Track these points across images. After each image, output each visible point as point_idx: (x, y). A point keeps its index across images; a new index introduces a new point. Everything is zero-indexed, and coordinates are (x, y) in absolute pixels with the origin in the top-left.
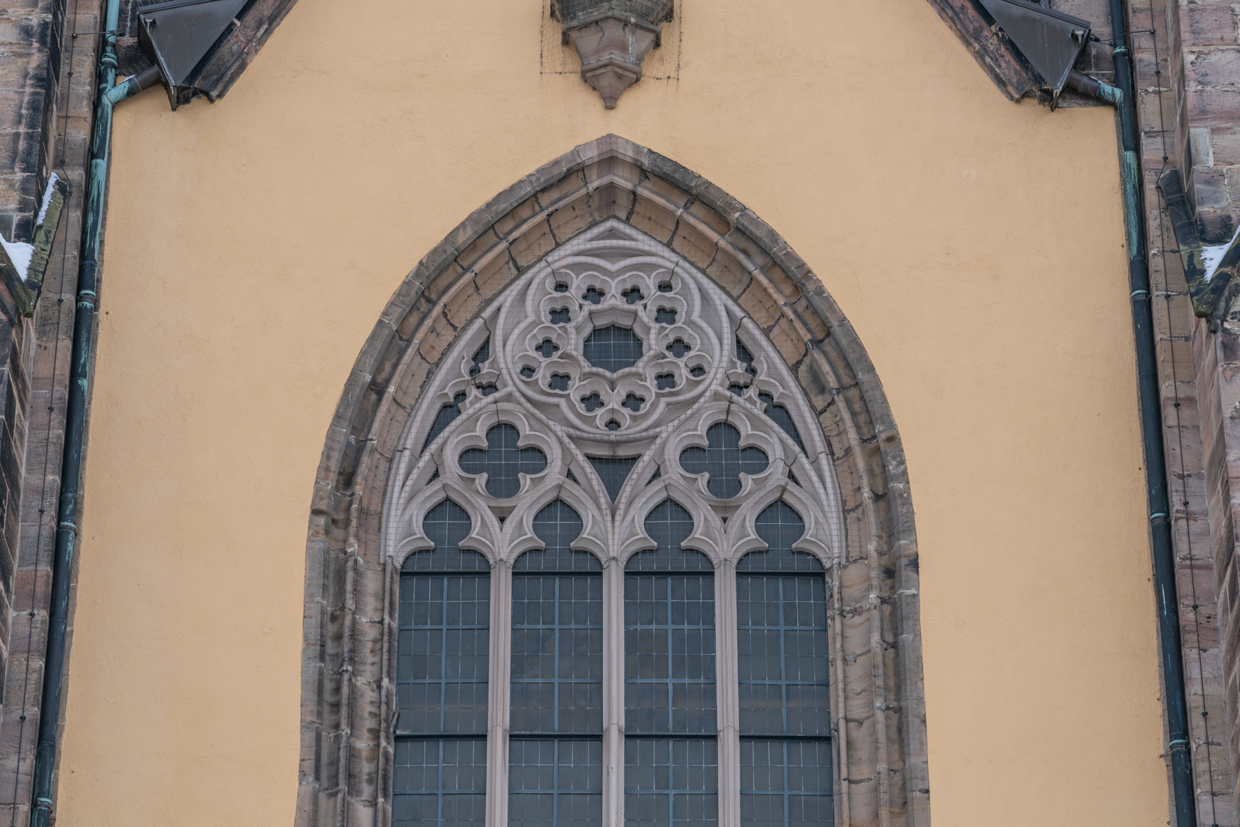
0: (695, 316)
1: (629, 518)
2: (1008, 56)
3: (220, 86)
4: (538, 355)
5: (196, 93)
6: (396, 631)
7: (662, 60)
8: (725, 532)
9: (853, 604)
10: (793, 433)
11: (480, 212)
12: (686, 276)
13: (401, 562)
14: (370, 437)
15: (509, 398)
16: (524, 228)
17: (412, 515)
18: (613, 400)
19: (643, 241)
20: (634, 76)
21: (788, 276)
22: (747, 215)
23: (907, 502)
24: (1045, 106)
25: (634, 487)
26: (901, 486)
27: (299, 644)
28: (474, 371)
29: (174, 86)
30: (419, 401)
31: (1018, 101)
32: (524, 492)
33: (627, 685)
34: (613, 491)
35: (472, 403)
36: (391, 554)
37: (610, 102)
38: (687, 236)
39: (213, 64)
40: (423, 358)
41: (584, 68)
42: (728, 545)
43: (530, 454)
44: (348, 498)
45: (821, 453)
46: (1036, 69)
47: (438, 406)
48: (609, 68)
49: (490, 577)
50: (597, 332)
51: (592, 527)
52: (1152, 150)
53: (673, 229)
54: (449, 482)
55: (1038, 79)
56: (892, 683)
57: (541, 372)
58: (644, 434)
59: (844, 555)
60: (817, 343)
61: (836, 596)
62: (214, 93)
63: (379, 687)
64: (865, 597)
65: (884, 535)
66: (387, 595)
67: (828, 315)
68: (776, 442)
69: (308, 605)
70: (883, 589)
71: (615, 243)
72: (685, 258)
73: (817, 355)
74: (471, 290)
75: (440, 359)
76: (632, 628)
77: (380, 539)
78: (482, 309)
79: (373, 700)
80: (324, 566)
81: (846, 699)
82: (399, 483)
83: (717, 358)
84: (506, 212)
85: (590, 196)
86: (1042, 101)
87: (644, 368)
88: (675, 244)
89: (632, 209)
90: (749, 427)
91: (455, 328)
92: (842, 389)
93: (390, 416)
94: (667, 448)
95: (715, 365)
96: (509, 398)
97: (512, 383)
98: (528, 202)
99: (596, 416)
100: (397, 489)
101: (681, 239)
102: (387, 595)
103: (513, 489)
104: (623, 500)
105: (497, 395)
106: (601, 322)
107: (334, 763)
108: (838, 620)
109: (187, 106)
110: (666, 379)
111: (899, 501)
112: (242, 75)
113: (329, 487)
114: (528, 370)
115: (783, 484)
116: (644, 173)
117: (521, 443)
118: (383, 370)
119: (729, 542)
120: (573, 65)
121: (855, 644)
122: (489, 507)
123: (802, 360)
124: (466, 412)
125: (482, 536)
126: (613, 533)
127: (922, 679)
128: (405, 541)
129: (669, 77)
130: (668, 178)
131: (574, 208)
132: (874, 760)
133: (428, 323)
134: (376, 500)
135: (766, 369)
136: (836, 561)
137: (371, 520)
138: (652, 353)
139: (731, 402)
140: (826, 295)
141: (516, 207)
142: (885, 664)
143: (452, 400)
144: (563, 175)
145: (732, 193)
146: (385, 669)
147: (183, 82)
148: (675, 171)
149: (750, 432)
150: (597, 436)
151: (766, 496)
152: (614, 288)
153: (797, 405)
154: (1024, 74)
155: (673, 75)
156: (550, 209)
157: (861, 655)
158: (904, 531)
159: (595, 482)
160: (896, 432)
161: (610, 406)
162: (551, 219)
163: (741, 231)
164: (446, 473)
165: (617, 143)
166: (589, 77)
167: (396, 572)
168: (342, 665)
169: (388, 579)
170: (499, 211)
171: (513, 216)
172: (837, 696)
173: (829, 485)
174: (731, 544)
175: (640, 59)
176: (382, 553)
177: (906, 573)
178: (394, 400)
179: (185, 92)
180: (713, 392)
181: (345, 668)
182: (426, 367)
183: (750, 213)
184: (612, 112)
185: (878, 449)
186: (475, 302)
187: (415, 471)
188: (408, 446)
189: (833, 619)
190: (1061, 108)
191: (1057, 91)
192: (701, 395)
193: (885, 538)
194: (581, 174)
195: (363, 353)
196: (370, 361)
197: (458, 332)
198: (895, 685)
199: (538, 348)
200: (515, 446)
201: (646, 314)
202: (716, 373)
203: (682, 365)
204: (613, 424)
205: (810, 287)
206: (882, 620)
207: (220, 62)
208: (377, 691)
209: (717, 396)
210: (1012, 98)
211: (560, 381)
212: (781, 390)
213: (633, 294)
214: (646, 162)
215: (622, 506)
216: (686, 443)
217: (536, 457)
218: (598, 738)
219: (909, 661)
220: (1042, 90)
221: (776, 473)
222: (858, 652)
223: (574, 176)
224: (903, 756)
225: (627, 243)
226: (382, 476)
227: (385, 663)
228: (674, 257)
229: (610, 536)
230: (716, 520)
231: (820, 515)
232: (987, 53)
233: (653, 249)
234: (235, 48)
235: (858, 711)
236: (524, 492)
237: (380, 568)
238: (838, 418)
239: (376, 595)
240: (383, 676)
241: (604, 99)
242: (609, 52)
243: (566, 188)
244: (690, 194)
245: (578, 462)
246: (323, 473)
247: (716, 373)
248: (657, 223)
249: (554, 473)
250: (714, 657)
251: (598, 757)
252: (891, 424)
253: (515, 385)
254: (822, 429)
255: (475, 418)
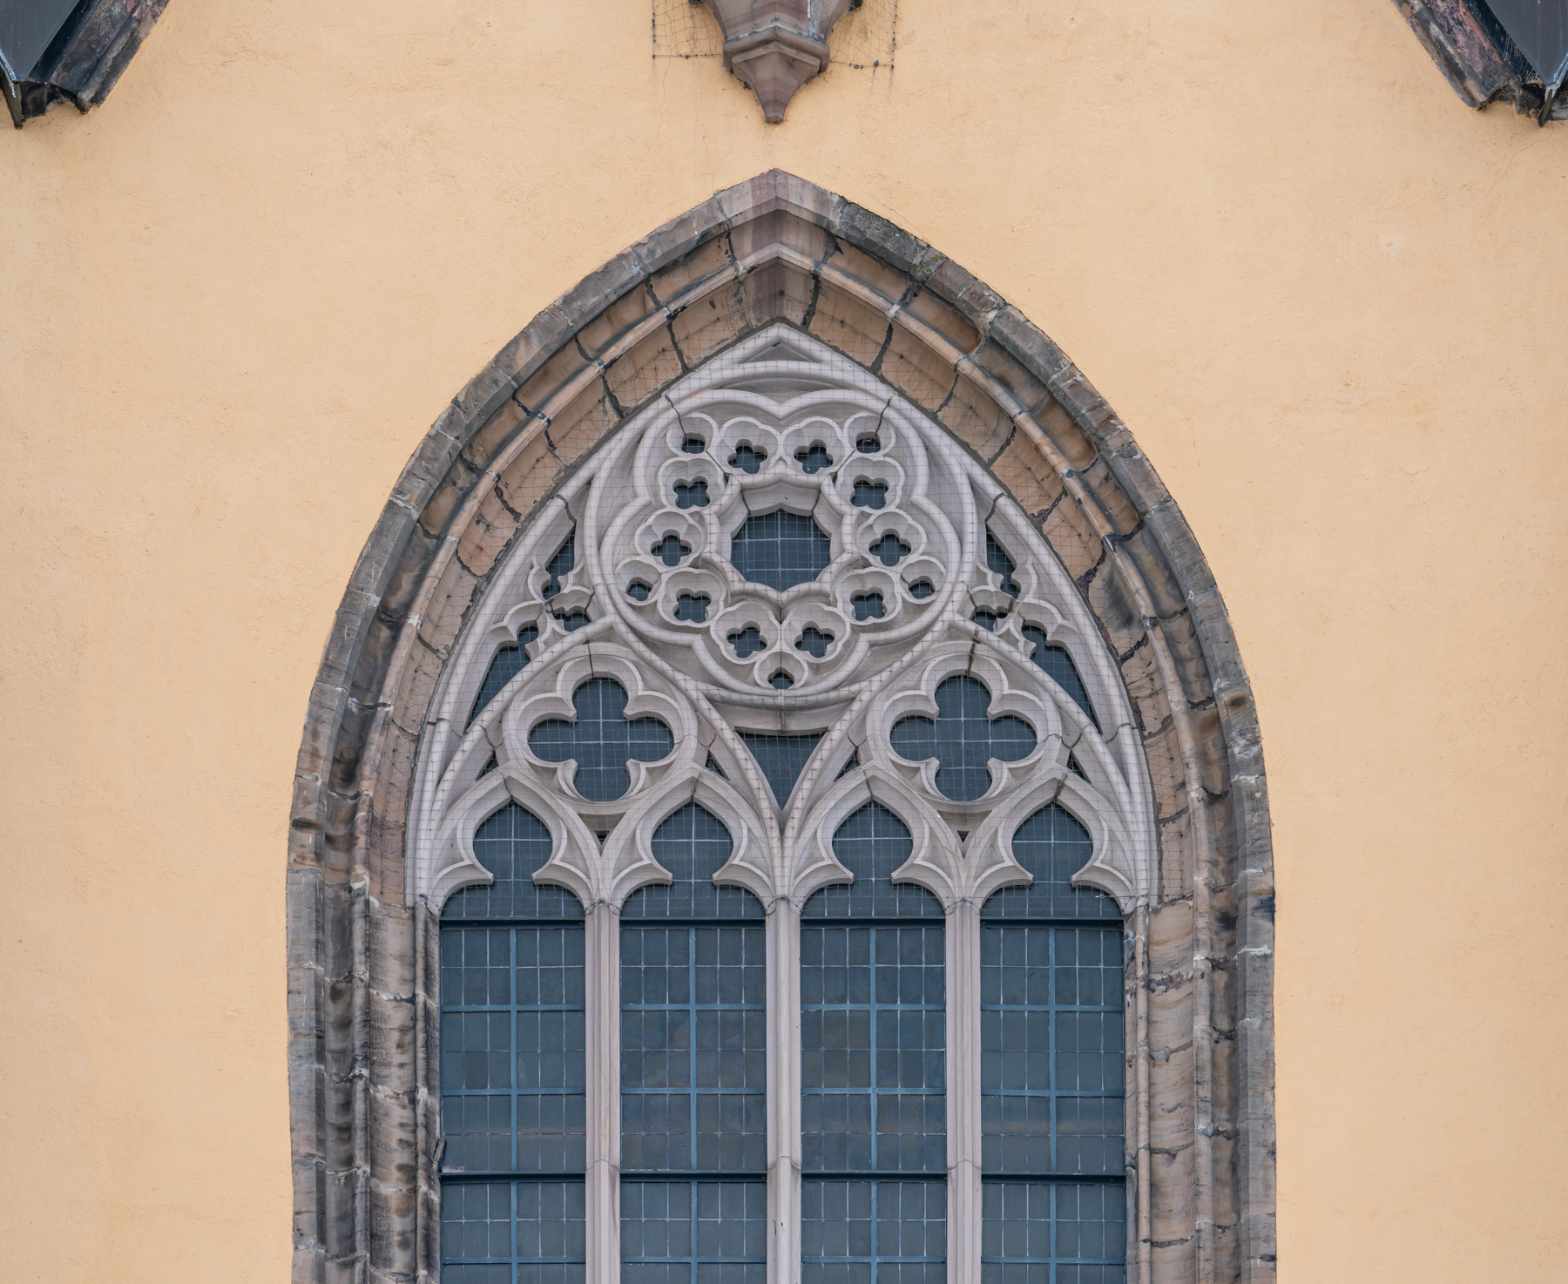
0: (919, 496)
1: (808, 833)
2: (1471, 24)
3: (96, 82)
4: (655, 562)
5: (57, 94)
6: (436, 1014)
7: (864, 31)
8: (964, 856)
9: (1167, 970)
10: (1078, 692)
11: (553, 311)
12: (903, 425)
13: (441, 905)
14: (381, 701)
15: (609, 635)
16: (629, 339)
17: (455, 829)
18: (782, 637)
19: (831, 363)
20: (816, 62)
21: (1075, 425)
22: (1009, 316)
23: (1261, 806)
24: (1528, 116)
25: (815, 782)
26: (1252, 780)
27: (283, 1035)
28: (550, 590)
29: (15, 83)
30: (461, 640)
31: (1482, 108)
32: (636, 791)
33: (806, 1098)
34: (782, 788)
35: (547, 644)
36: (423, 891)
37: (774, 110)
38: (905, 354)
39: (81, 42)
40: (464, 567)
41: (730, 46)
42: (968, 877)
43: (646, 728)
44: (351, 802)
45: (1123, 725)
46: (1517, 46)
47: (492, 648)
48: (772, 47)
49: (584, 929)
50: (754, 522)
51: (749, 847)
53: (882, 341)
54: (515, 775)
55: (1520, 66)
56: (1224, 1093)
57: (662, 589)
58: (833, 695)
59: (1155, 891)
60: (1121, 539)
61: (1140, 958)
62: (86, 96)
63: (413, 1101)
64: (1187, 959)
65: (1221, 859)
66: (420, 956)
67: (1142, 491)
68: (1049, 707)
69: (294, 973)
70: (1217, 946)
71: (783, 366)
72: (902, 393)
73: (1121, 560)
74: (541, 449)
75: (493, 569)
76: (813, 1008)
77: (405, 868)
78: (560, 483)
79: (405, 1121)
80: (317, 911)
81: (1151, 1118)
82: (432, 777)
83: (954, 567)
84: (597, 312)
85: (741, 283)
86: (1525, 107)
87: (833, 583)
88: (887, 368)
89: (813, 306)
90: (1006, 683)
91: (516, 515)
92: (1160, 618)
93: (413, 666)
94: (869, 717)
95: (951, 577)
96: (609, 635)
97: (613, 609)
98: (635, 293)
99: (754, 664)
100: (429, 787)
101: (896, 359)
102: (420, 956)
103: (618, 786)
104: (799, 804)
105: (589, 629)
106: (761, 505)
107: (347, 1216)
108: (1142, 995)
109: (41, 119)
110: (868, 602)
111: (1247, 805)
112: (132, 62)
113: (319, 783)
114: (639, 588)
115: (1059, 776)
116: (833, 241)
117: (630, 711)
118: (399, 587)
119: (969, 872)
120: (709, 41)
121: (1168, 1033)
122: (580, 815)
123: (1095, 570)
124: (539, 659)
125: (569, 863)
126: (783, 858)
127: (1273, 1088)
128: (446, 871)
129: (876, 64)
130: (875, 249)
131: (713, 305)
132: (1192, 1211)
133: (471, 506)
134: (396, 804)
135: (1035, 586)
136: (1141, 902)
137: (389, 837)
138: (845, 557)
139: (976, 641)
140: (1137, 457)
141: (614, 303)
142: (1214, 1064)
143: (515, 638)
144: (694, 245)
145: (983, 277)
146: (421, 1073)
147: (30, 75)
148: (886, 237)
149: (1007, 691)
150: (755, 697)
151: (1031, 797)
152: (782, 447)
153: (1085, 645)
154: (1496, 57)
155: (884, 59)
156: (673, 307)
157: (1176, 1051)
158: (1253, 854)
159: (751, 775)
160: (1246, 690)
161: (776, 649)
162: (674, 323)
163: (998, 344)
164: (508, 760)
165: (786, 186)
167: (433, 921)
168: (352, 1068)
169: (420, 933)
170: (585, 309)
171: (609, 319)
172: (1138, 1114)
173: (1134, 779)
174: (973, 874)
175: (826, 30)
176: (409, 890)
177: (1254, 920)
178: (420, 638)
179: (36, 94)
180: (946, 625)
181: (357, 1072)
182: (469, 582)
183: (1013, 312)
184: (778, 129)
185: (1216, 719)
186: (548, 472)
187: (459, 757)
188: (445, 716)
189: (1134, 994)
190: (1557, 119)
191: (1552, 89)
192: (927, 629)
193: (1222, 865)
194: (724, 243)
195: (365, 558)
196: (377, 573)
197: (524, 521)
198: (1230, 1097)
199: (657, 550)
200: (621, 716)
201: (837, 495)
202: (952, 593)
203: (896, 578)
204: (781, 678)
205: (1113, 443)
206: (1212, 995)
207: (93, 38)
208: (409, 1107)
209: (953, 631)
210: (1472, 102)
211: (693, 605)
212: (1060, 620)
213: (813, 455)
214: (836, 219)
215: (797, 814)
216: (902, 709)
218: (760, 1178)
219: (1252, 1060)
220: (1525, 87)
221: (1048, 759)
222: (1173, 1046)
223: (714, 246)
224: (1238, 1203)
225: (804, 367)
226: (403, 765)
227: (421, 1064)
228: (884, 391)
229: (777, 862)
230: (949, 836)
231: (1118, 827)
232: (1434, 16)
233: (848, 377)
234: (117, 10)
235: (1169, 1135)
236: (636, 791)
237: (406, 915)
238: (1152, 668)
239: (401, 957)
240: (419, 1084)
241: (764, 104)
242: (772, 16)
243: (699, 268)
244: (912, 278)
245: (723, 741)
246: (307, 759)
247: (952, 593)
248: (855, 331)
249: (685, 760)
250: (943, 1055)
251: (760, 1208)
252: (1240, 678)
253: (618, 612)
254: (1126, 686)
255: (554, 668)
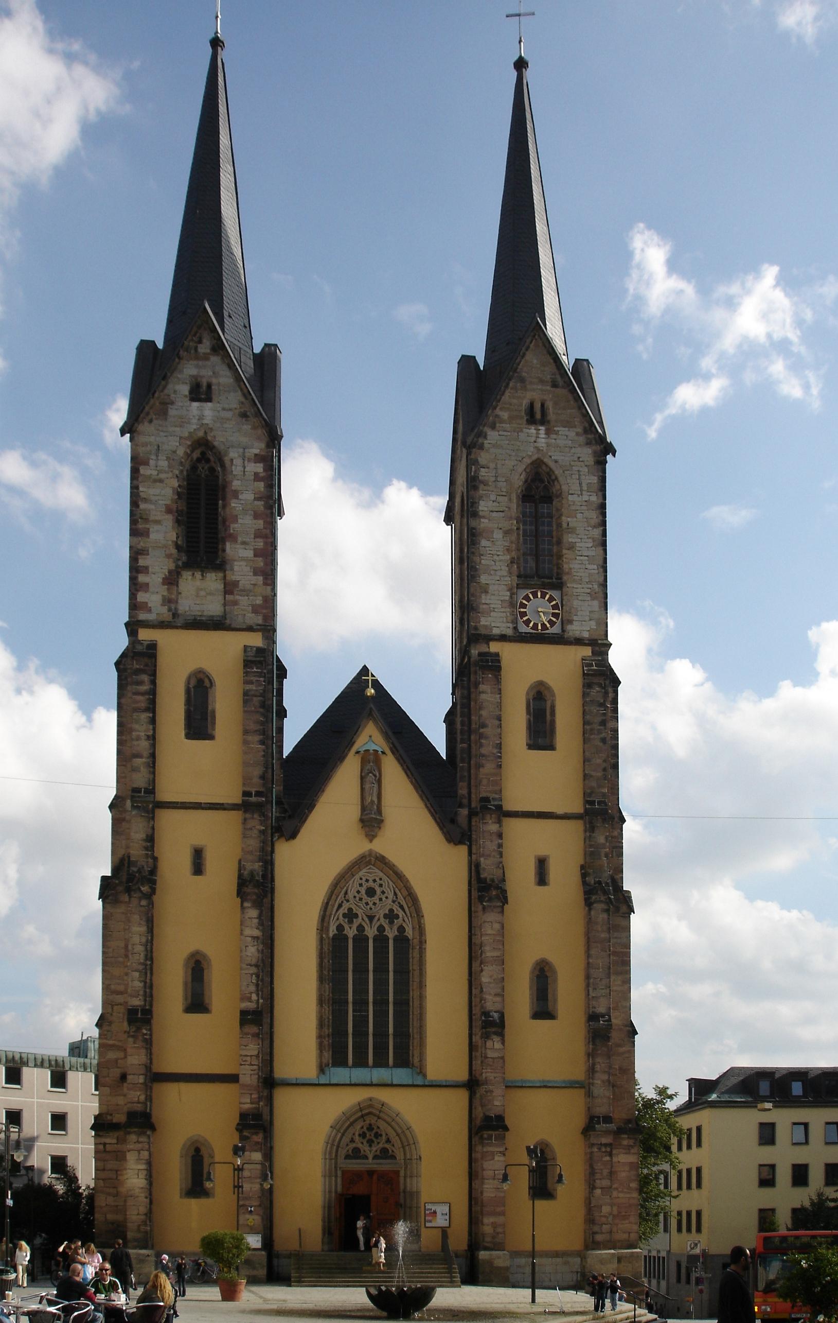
28: (345, 897)
52: (474, 857)
110: (381, 900)
166: (367, 836)
211: (361, 899)
217: (356, 916)
221: (400, 919)
230: (390, 930)
